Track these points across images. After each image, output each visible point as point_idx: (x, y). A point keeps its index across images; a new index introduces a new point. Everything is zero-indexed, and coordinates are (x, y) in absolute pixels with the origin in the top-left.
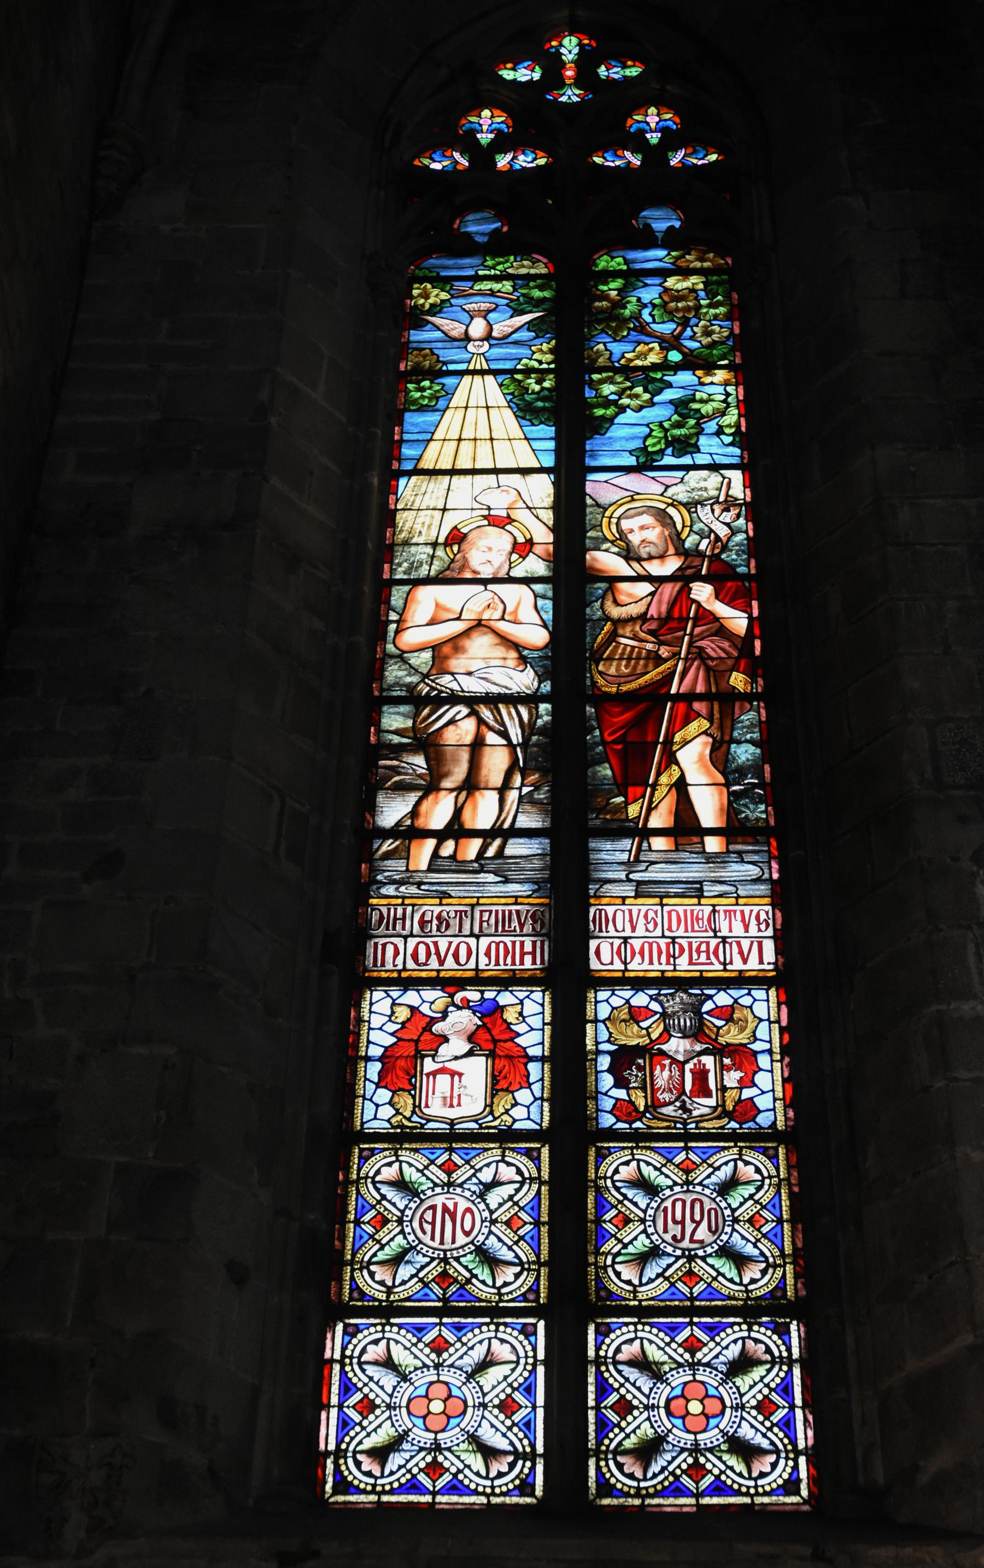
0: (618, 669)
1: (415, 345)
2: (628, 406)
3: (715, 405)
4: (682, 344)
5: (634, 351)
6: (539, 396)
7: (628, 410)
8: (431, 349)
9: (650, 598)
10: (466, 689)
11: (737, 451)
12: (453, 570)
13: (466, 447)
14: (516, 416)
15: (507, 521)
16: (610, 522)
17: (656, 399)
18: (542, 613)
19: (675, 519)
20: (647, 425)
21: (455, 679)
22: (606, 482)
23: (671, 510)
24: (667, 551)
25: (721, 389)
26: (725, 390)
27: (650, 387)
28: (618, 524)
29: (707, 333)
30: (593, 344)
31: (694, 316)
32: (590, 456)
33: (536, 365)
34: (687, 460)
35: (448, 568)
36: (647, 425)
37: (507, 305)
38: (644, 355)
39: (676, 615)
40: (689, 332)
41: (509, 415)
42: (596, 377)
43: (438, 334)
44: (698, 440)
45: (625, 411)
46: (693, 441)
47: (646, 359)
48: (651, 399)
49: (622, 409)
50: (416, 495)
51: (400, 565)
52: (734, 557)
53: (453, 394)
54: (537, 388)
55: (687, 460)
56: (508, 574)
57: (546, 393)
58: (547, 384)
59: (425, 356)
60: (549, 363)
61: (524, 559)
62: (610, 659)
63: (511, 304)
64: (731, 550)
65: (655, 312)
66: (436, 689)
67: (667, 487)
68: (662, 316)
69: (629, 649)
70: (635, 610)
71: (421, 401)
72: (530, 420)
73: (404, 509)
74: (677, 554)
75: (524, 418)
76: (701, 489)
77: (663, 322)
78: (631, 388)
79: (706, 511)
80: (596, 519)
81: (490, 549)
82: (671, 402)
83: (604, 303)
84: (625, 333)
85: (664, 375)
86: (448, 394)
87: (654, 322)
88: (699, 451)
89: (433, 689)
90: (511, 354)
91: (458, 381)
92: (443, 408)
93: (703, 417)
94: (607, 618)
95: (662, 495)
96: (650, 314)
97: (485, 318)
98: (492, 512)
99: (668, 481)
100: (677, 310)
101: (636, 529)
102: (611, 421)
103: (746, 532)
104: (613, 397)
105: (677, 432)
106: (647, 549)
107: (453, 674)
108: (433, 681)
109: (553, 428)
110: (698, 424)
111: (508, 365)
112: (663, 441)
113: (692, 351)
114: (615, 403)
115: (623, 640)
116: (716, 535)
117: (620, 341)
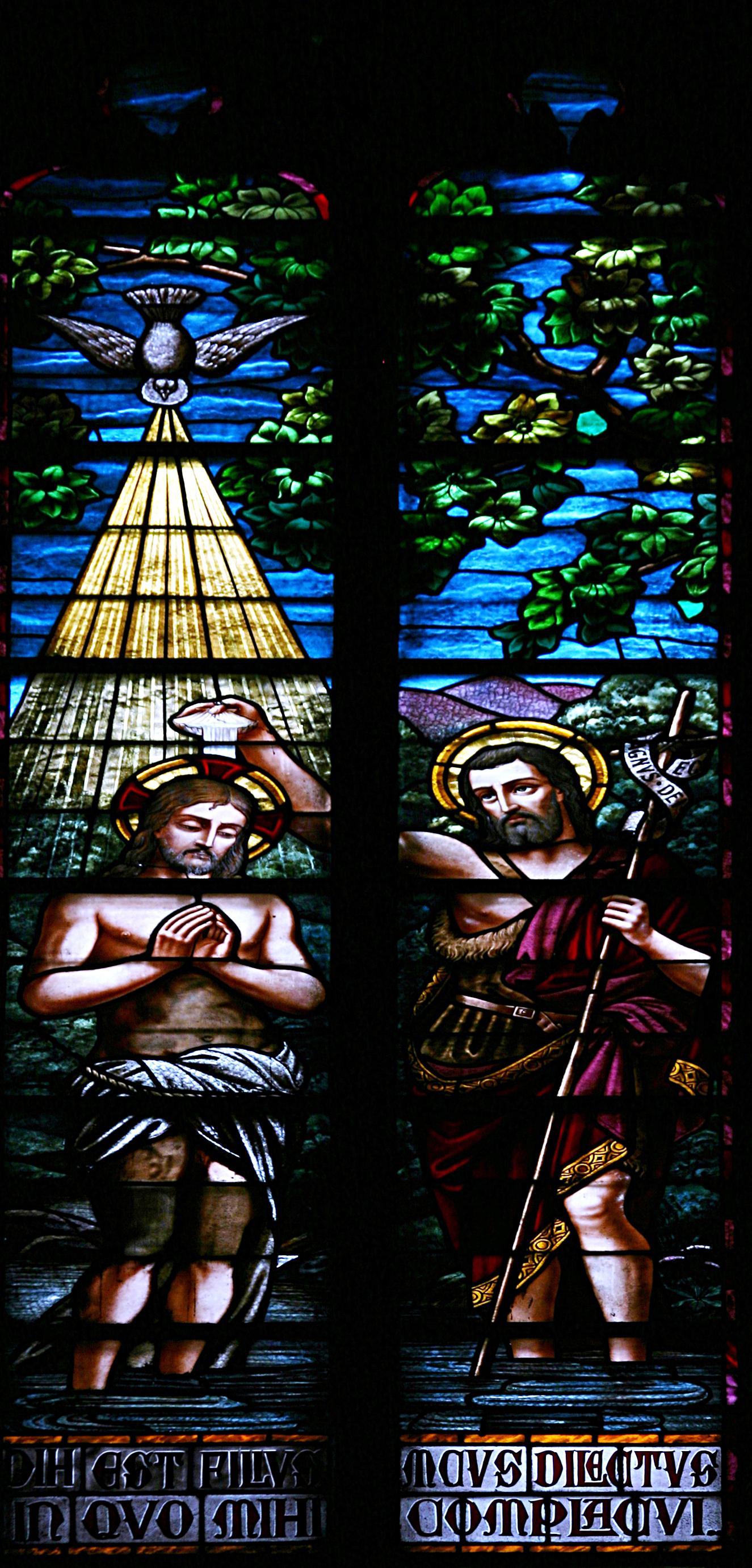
0: (458, 1052)
1: (25, 383)
2: (490, 532)
3: (670, 533)
4: (608, 396)
5: (503, 410)
6: (300, 504)
7: (488, 541)
8: (61, 393)
9: (522, 922)
10: (165, 1085)
11: (713, 634)
12: (131, 864)
13: (147, 617)
14: (252, 551)
15: (237, 768)
16: (446, 776)
17: (550, 518)
18: (311, 948)
19: (579, 771)
20: (528, 575)
21: (145, 1068)
22: (441, 692)
23: (573, 755)
24: (560, 832)
25: (683, 500)
26: (694, 501)
27: (536, 491)
28: (464, 779)
29: (662, 371)
30: (415, 391)
31: (636, 333)
32: (407, 638)
33: (291, 433)
34: (607, 651)
35: (121, 859)
36: (528, 575)
37: (225, 293)
38: (524, 419)
39: (573, 953)
40: (623, 370)
41: (234, 544)
42: (420, 468)
43: (74, 358)
44: (632, 610)
45: (482, 545)
46: (621, 613)
47: (530, 429)
48: (539, 517)
49: (477, 538)
50: (49, 712)
51: (24, 851)
52: (692, 846)
53: (116, 497)
54: (296, 486)
55: (607, 651)
56: (242, 870)
57: (315, 498)
58: (315, 480)
59: (49, 407)
60: (320, 434)
61: (274, 846)
62: (442, 1037)
63: (235, 292)
64: (687, 834)
65: (552, 321)
66: (110, 1085)
67: (564, 706)
68: (564, 331)
69: (479, 1016)
70: (489, 942)
71: (46, 511)
72: (280, 559)
73: (23, 742)
74: (579, 842)
75: (268, 553)
76: (632, 710)
77: (570, 346)
78: (497, 493)
79: (640, 756)
80: (420, 766)
81: (205, 824)
82: (579, 525)
83: (441, 296)
84: (486, 369)
85: (566, 467)
86: (103, 496)
87: (549, 344)
88: (633, 633)
89: (100, 1085)
90: (238, 408)
91: (124, 468)
92: (94, 527)
93: (644, 559)
94: (440, 958)
95: (553, 721)
96: (541, 326)
97: (177, 325)
98: (207, 751)
99: (564, 694)
100: (602, 316)
101: (499, 791)
102: (451, 562)
103: (720, 798)
104: (456, 512)
105: (590, 591)
106: (520, 828)
107: (139, 1058)
108: (101, 1070)
109: (331, 577)
110: (633, 575)
111: (231, 435)
112: (559, 610)
113: (628, 410)
114: (461, 523)
115: (470, 1000)
116: (658, 802)
117: (473, 386)
